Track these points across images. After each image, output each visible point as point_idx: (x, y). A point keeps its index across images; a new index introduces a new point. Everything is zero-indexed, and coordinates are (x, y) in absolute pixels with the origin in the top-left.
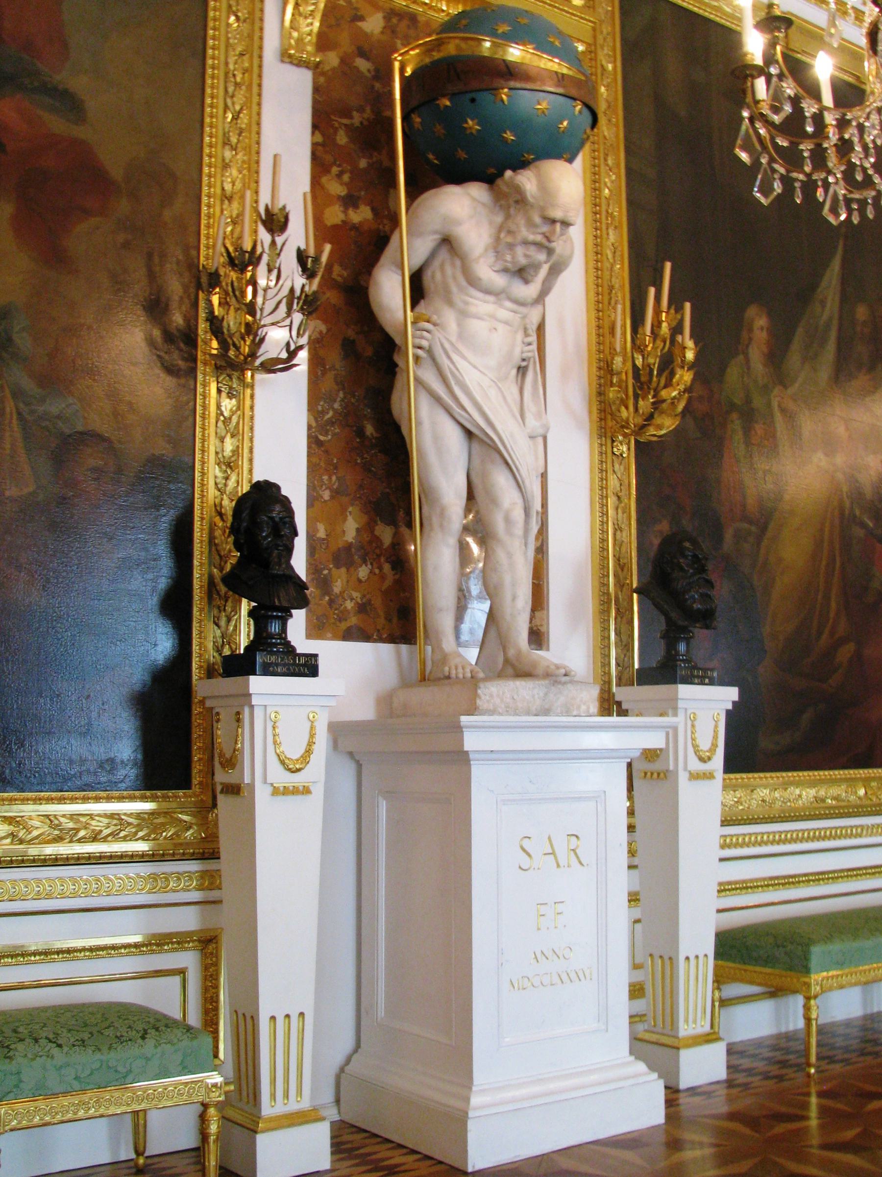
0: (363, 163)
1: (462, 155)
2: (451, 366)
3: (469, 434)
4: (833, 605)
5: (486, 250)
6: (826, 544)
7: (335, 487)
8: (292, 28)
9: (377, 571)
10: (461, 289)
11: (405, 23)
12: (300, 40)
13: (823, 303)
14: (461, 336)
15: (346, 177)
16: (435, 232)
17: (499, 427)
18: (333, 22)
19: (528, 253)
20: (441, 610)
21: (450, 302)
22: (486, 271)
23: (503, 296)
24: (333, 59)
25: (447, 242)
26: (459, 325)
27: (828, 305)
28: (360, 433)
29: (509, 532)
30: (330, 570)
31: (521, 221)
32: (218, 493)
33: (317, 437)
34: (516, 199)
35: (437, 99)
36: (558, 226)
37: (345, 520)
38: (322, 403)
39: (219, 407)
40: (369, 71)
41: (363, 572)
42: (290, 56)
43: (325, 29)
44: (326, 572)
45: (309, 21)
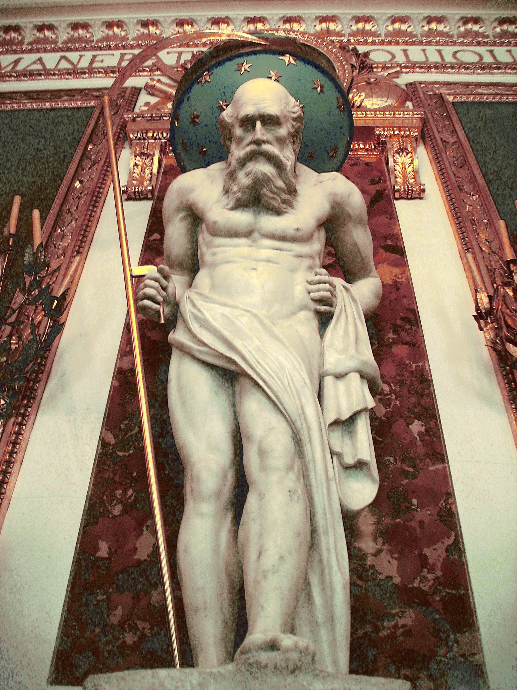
2: (195, 311)
7: (130, 501)
14: (213, 287)
19: (248, 170)
23: (256, 235)
26: (212, 277)
29: (263, 468)
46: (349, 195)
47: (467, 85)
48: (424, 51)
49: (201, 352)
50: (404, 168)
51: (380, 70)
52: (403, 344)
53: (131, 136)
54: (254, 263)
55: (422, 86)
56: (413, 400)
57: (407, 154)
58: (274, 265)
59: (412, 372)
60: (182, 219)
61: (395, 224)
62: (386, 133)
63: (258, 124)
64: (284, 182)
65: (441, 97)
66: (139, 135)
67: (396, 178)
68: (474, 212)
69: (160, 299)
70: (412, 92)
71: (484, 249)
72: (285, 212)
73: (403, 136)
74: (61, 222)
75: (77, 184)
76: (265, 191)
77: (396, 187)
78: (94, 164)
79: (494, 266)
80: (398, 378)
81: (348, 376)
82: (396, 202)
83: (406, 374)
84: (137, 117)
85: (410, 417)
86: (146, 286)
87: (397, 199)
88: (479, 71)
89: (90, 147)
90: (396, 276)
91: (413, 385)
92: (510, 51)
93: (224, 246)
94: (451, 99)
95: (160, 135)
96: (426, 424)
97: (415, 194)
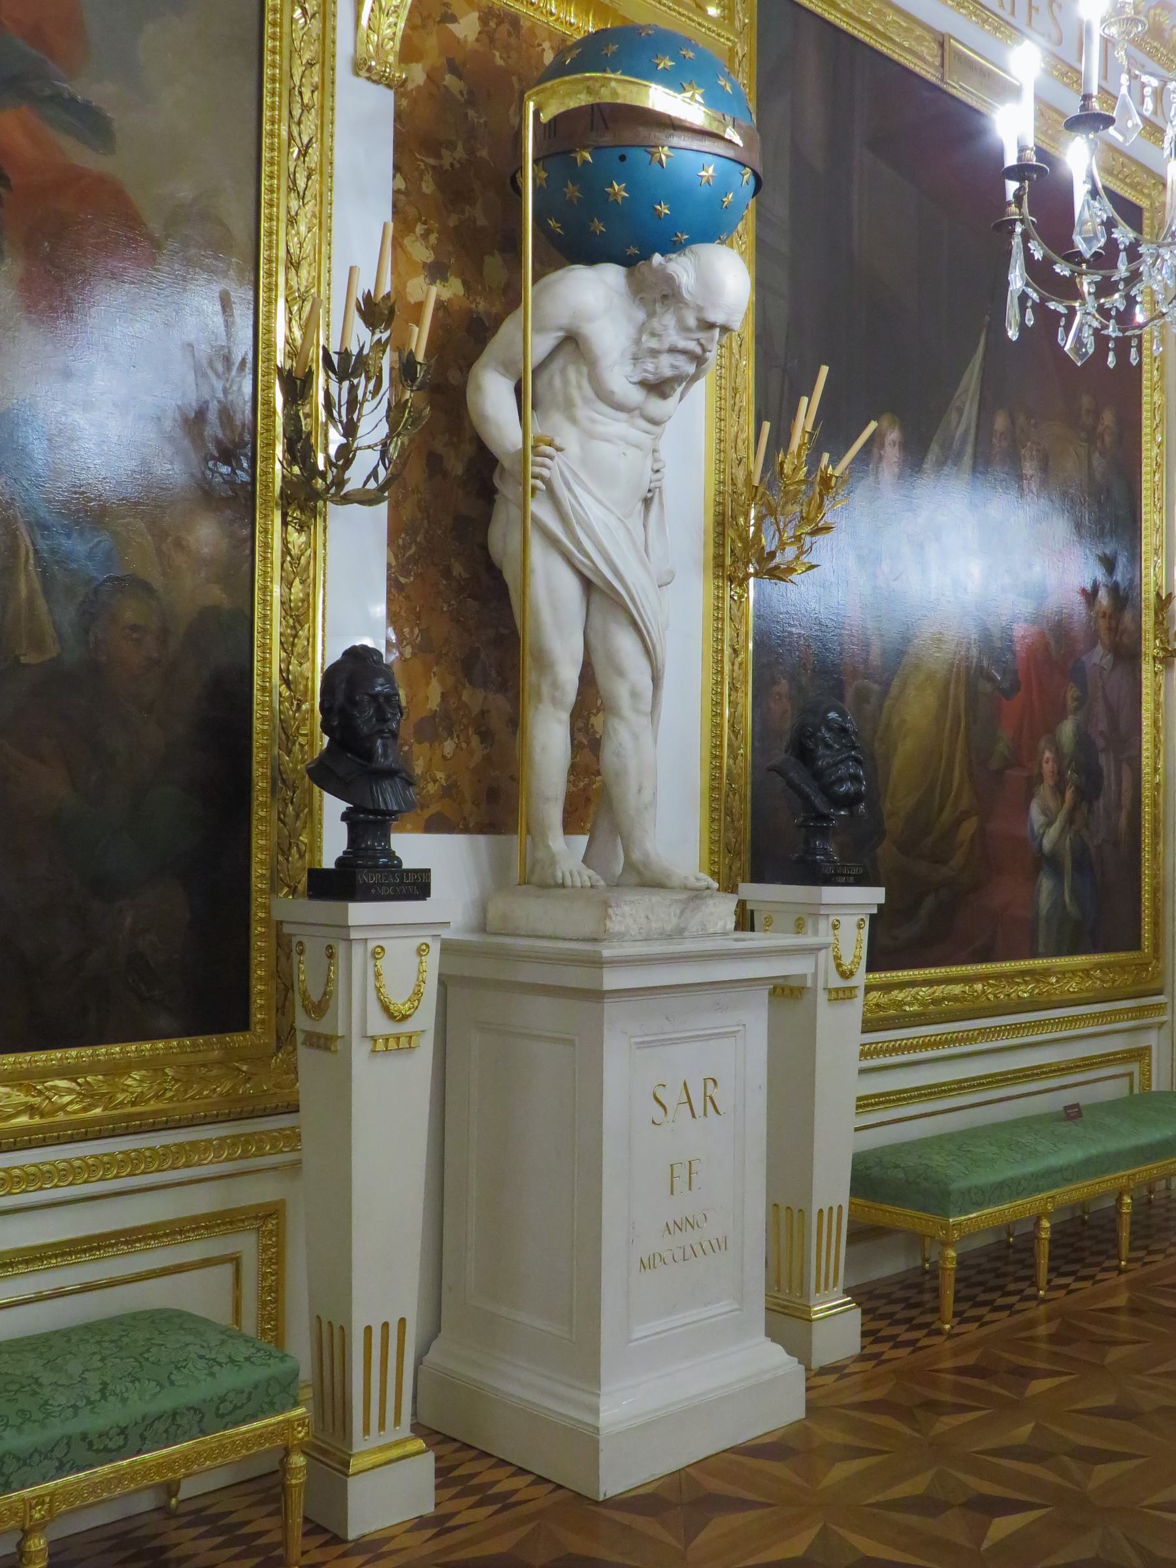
0: (453, 221)
1: (599, 227)
3: (588, 585)
4: (957, 774)
5: (622, 355)
6: (951, 702)
8: (370, 27)
9: (464, 745)
10: (586, 401)
11: (505, 27)
12: (379, 47)
13: (960, 412)
15: (433, 238)
16: (560, 329)
17: (629, 579)
18: (419, 22)
19: (676, 363)
20: (548, 799)
21: (574, 421)
22: (620, 379)
23: (637, 412)
24: (417, 74)
25: (572, 342)
27: (965, 414)
28: (447, 573)
30: (411, 746)
31: (669, 320)
32: (284, 654)
33: (397, 580)
34: (664, 293)
35: (574, 151)
36: (717, 331)
37: (428, 684)
39: (285, 542)
40: (461, 92)
41: (449, 747)
42: (369, 69)
43: (409, 32)
44: (406, 748)
45: (392, 19)
49: (582, 562)
93: (605, 416)
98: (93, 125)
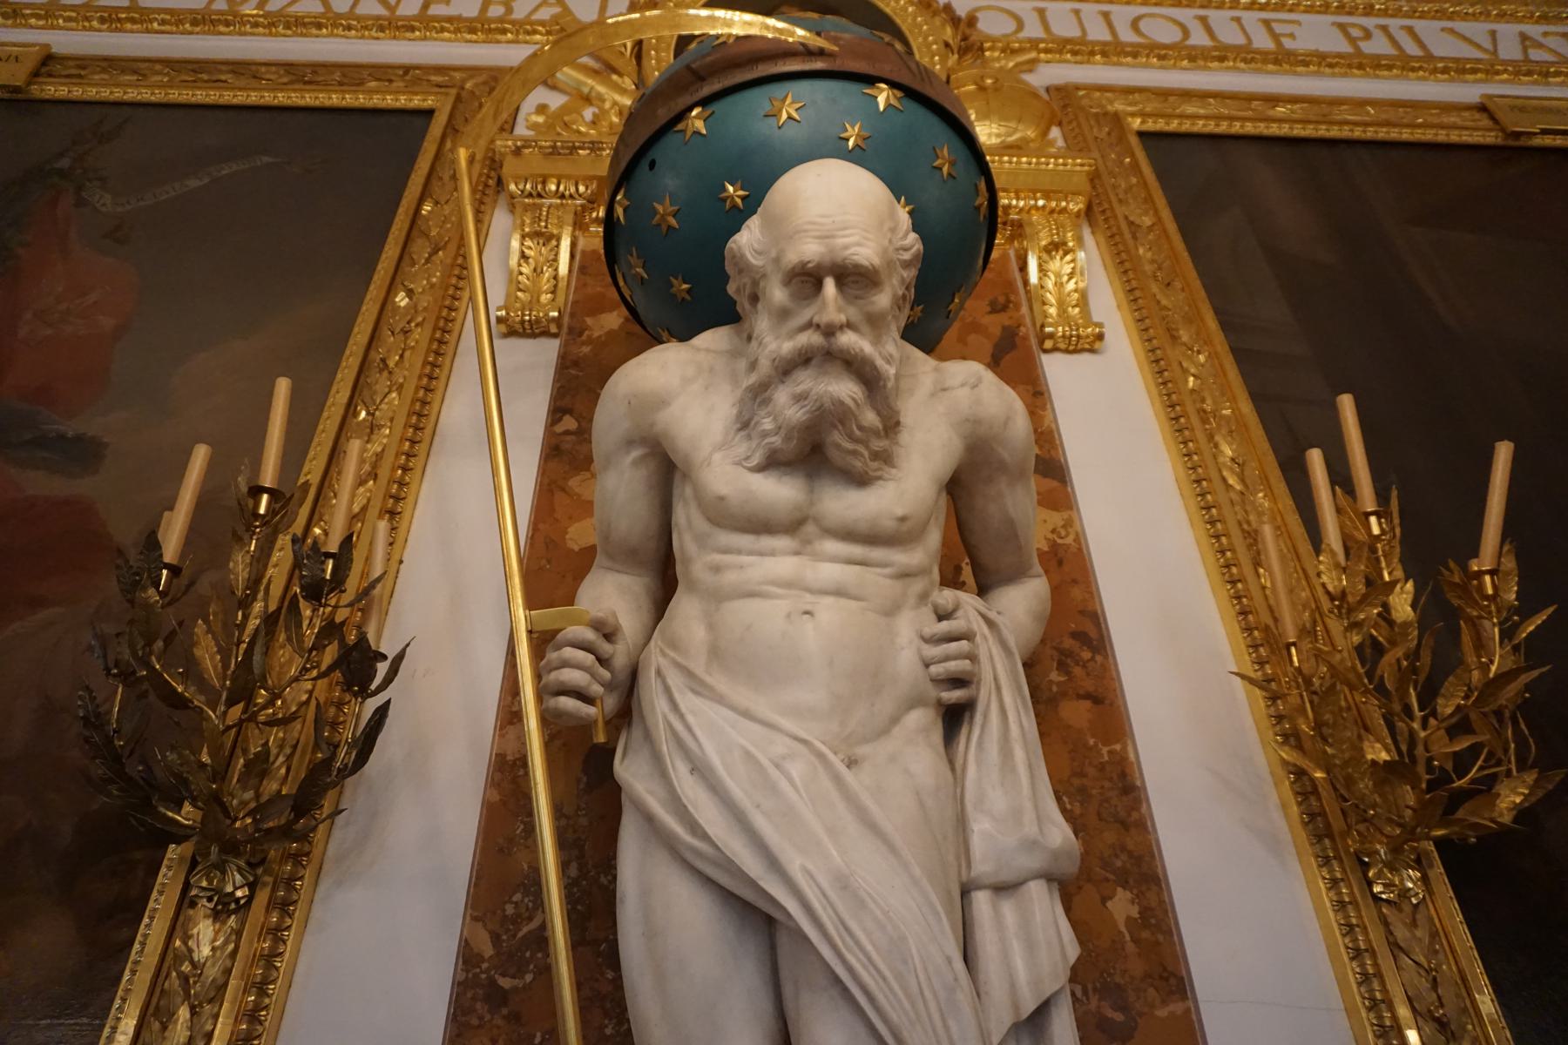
14: (715, 653)
19: (799, 389)
22: (727, 473)
23: (810, 528)
26: (711, 627)
33: (492, 983)
38: (517, 897)
46: (1007, 420)
47: (1164, 94)
48: (1077, 12)
49: (698, 853)
50: (1059, 285)
51: (996, 54)
52: (1080, 697)
53: (512, 187)
54: (808, 597)
55: (1081, 93)
56: (1110, 836)
57: (1066, 253)
58: (853, 604)
59: (1102, 767)
60: (635, 463)
61: (1044, 408)
62: (1022, 203)
63: (830, 286)
64: (879, 414)
65: (1117, 120)
66: (528, 186)
67: (1044, 303)
68: (1206, 394)
69: (597, 689)
70: (1063, 105)
71: (1231, 482)
72: (879, 478)
73: (1052, 211)
74: (366, 393)
75: (401, 300)
76: (837, 437)
77: (1048, 330)
78: (435, 252)
79: (1254, 525)
80: (1076, 782)
81: (1025, 887)
82: (1045, 358)
83: (1091, 771)
84: (524, 147)
85: (1107, 880)
86: (565, 664)
87: (1046, 351)
88: (1185, 62)
89: (427, 208)
90: (1053, 531)
91: (1107, 800)
92: (1238, 20)
93: (739, 552)
94: (1136, 123)
95: (573, 190)
96: (1139, 897)
97: (1087, 343)
98: (83, 453)
